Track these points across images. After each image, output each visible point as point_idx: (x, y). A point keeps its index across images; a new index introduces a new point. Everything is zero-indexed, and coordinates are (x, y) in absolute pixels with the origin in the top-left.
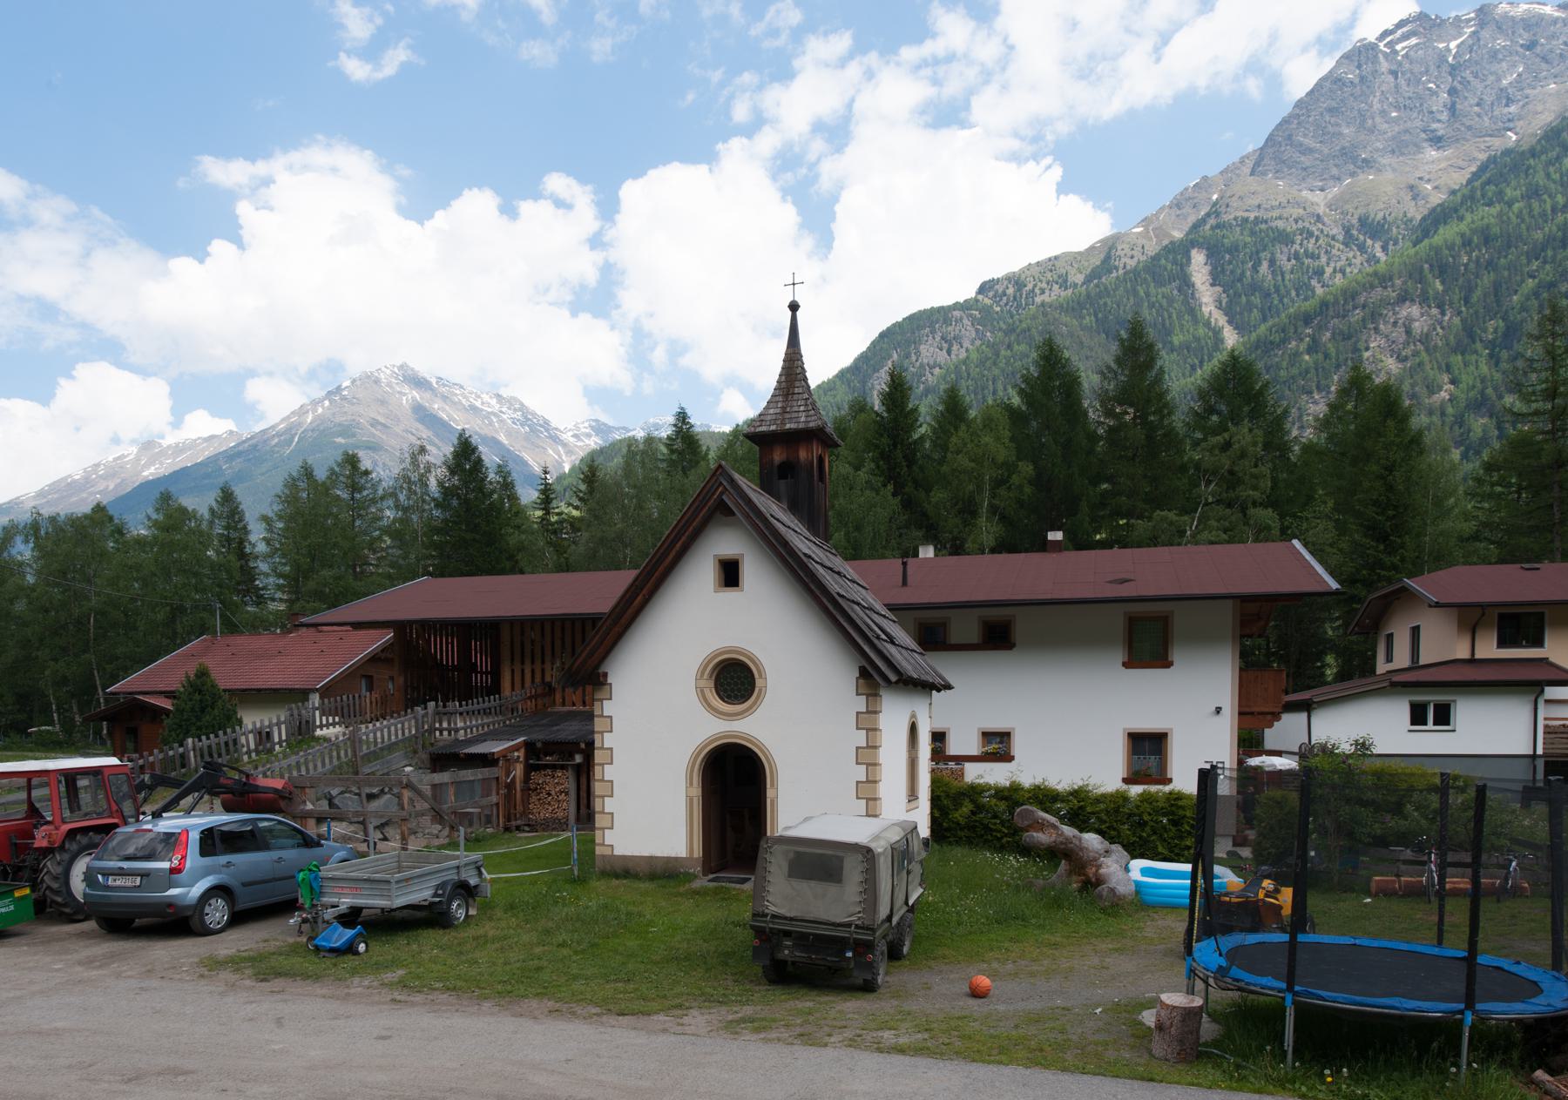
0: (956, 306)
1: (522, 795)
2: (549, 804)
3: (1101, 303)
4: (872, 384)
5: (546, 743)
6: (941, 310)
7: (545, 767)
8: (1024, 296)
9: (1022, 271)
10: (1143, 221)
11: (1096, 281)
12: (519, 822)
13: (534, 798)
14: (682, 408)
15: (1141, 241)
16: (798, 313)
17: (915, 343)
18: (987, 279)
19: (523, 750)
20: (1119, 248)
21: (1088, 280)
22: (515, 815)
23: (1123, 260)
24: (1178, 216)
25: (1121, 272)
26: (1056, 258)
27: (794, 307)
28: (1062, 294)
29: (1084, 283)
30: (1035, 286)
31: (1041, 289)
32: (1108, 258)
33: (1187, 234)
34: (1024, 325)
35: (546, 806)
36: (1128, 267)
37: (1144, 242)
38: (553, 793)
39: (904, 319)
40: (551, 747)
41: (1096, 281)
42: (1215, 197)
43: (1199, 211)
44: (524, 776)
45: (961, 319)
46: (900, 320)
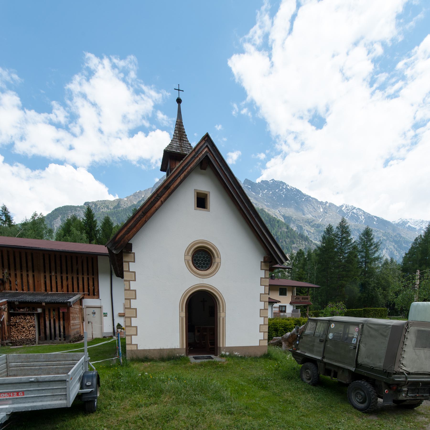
0: (78, 207)
1: (8, 328)
2: (24, 332)
3: (118, 215)
4: (54, 223)
5: (20, 303)
6: (73, 206)
7: (19, 314)
8: (97, 208)
9: (96, 202)
10: (126, 197)
11: (116, 209)
12: (7, 341)
13: (14, 329)
14: (5, 205)
15: (127, 202)
16: (181, 104)
17: (66, 214)
18: (87, 201)
19: (6, 305)
20: (121, 202)
21: (114, 208)
22: (5, 337)
23: (123, 206)
24: (135, 198)
25: (122, 208)
26: (105, 201)
27: (179, 101)
28: (108, 210)
29: (113, 209)
30: (100, 207)
31: (102, 208)
32: (118, 204)
33: (137, 203)
34: (98, 216)
35: (22, 333)
36: (124, 208)
37: (127, 202)
38: (26, 327)
39: (62, 207)
40: (23, 304)
41: (116, 209)
42: (143, 196)
43: (140, 198)
44: (8, 319)
45: (80, 210)
46: (61, 206)
